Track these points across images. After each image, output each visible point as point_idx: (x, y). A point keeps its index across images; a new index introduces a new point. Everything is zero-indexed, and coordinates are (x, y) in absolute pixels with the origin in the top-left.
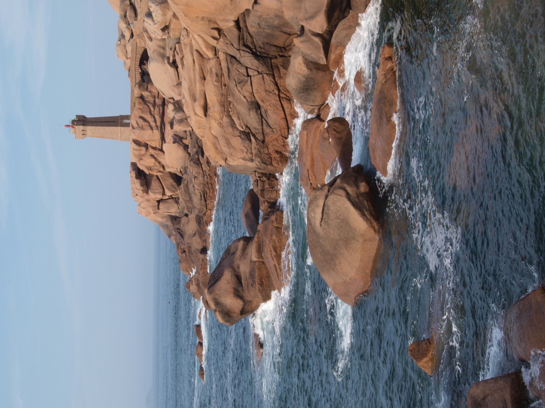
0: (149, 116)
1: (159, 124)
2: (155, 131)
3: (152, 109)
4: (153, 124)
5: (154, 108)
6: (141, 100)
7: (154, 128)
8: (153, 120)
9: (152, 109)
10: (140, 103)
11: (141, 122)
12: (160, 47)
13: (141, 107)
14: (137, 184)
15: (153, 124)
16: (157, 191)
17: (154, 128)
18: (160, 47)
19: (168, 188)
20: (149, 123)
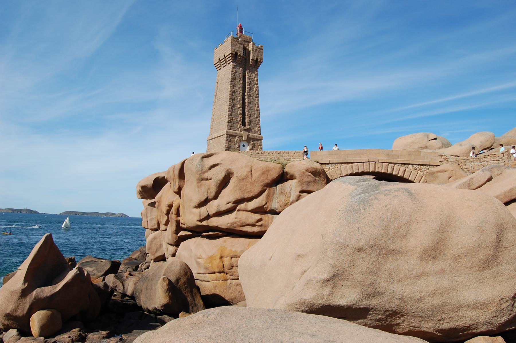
0: (232, 198)
1: (214, 222)
2: (197, 210)
3: (252, 205)
4: (213, 207)
5: (254, 211)
6: (274, 175)
7: (204, 211)
8: (224, 208)
9: (252, 205)
10: (266, 172)
11: (218, 175)
12: (445, 228)
13: (256, 175)
14: (150, 182)
15: (213, 207)
16: (149, 218)
17: (204, 211)
18: (445, 228)
19: (155, 238)
20: (216, 197)
